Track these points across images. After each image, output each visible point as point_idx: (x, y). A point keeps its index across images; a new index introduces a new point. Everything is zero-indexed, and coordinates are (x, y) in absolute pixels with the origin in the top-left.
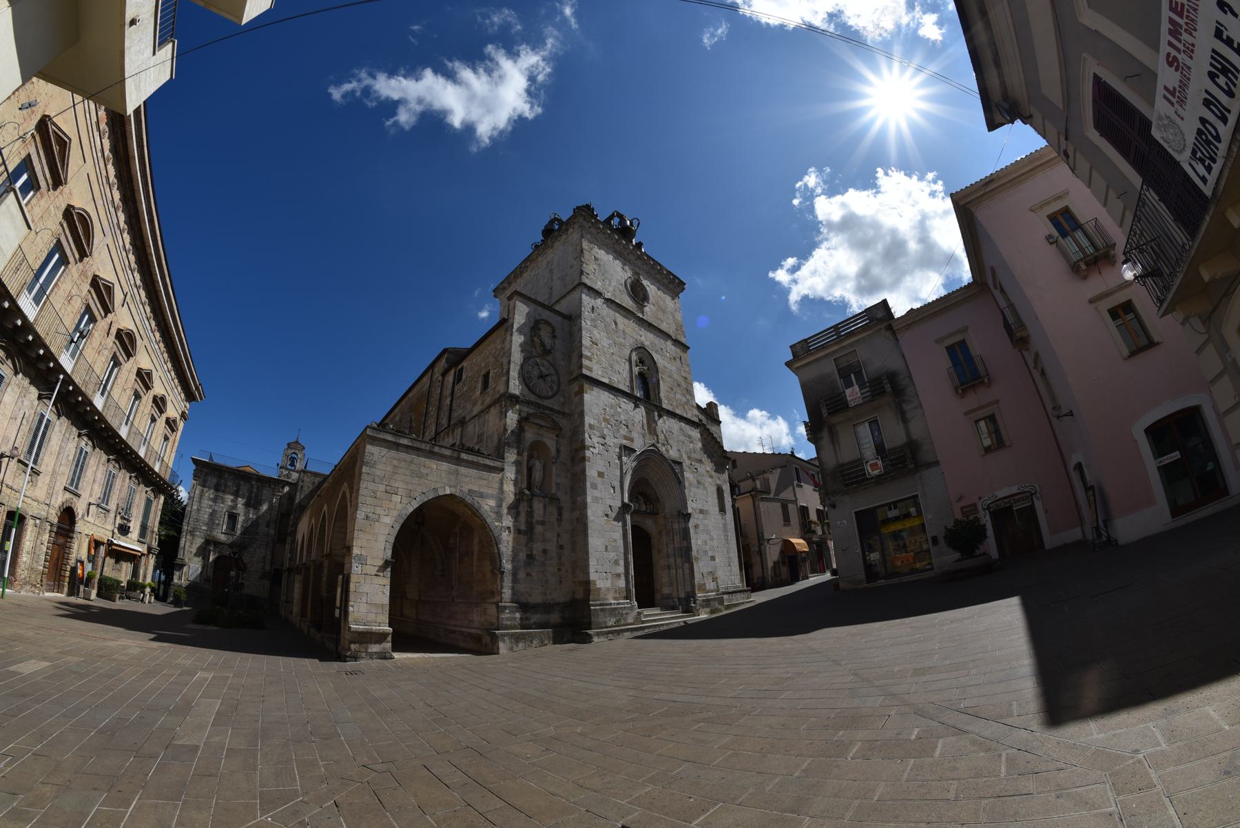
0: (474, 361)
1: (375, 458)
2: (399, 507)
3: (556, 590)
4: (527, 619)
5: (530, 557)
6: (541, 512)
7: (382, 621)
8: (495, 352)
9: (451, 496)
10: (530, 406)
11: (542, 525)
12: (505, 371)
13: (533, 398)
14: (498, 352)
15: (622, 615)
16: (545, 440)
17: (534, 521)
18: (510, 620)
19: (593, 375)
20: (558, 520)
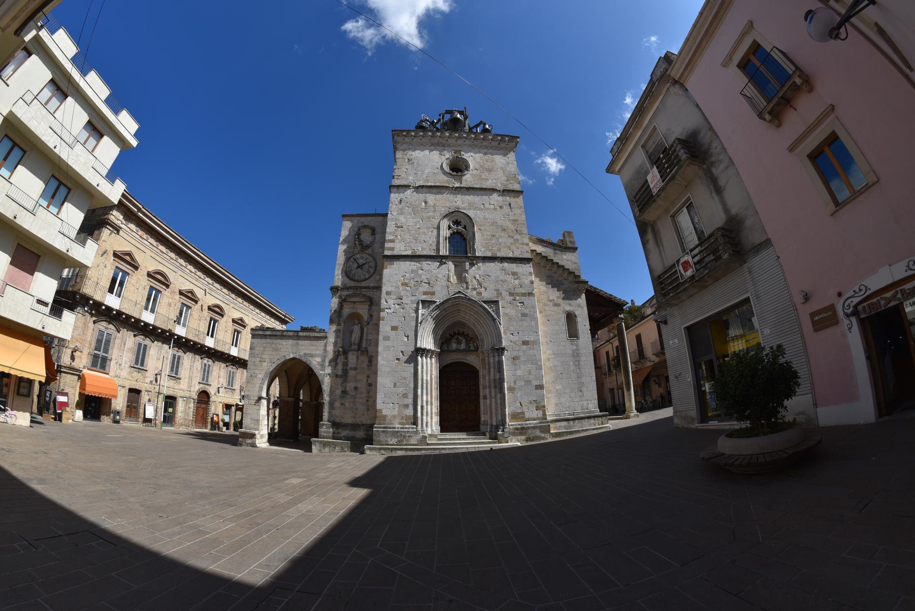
2: (266, 368)
3: (363, 415)
4: (338, 433)
5: (344, 392)
6: (355, 361)
9: (294, 359)
10: (350, 290)
11: (355, 370)
13: (352, 284)
15: (405, 437)
16: (359, 311)
17: (348, 368)
18: (326, 433)
19: (396, 253)
20: (368, 365)
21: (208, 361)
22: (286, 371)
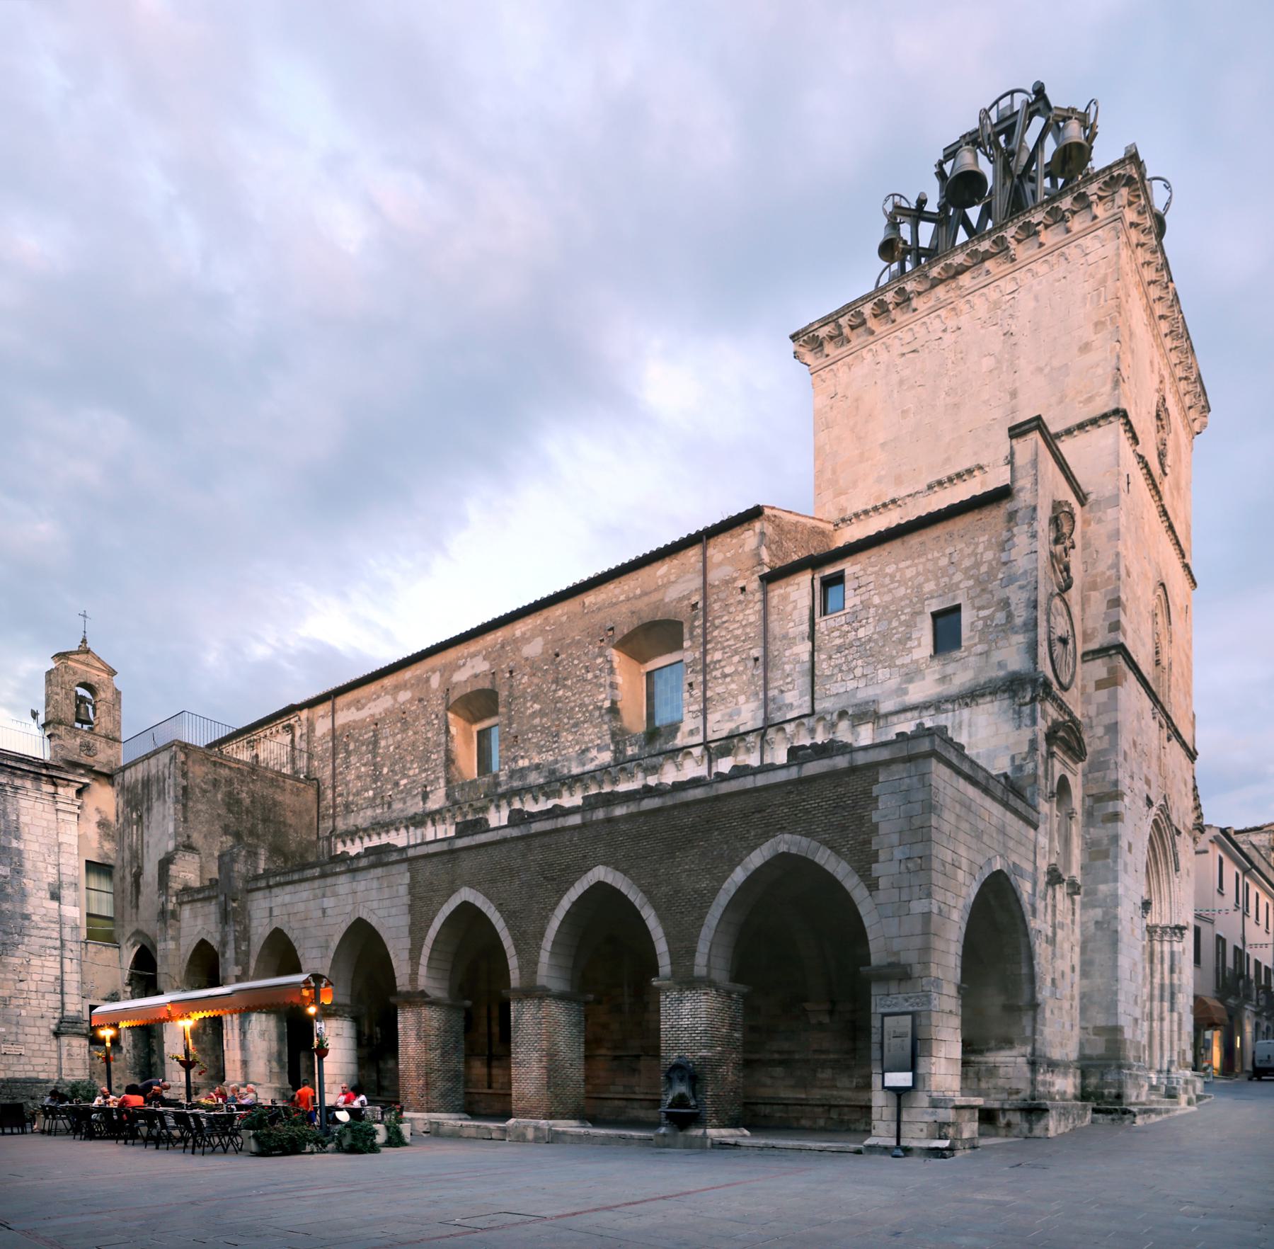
0: (890, 569)
8: (977, 565)
12: (1018, 621)
14: (984, 569)
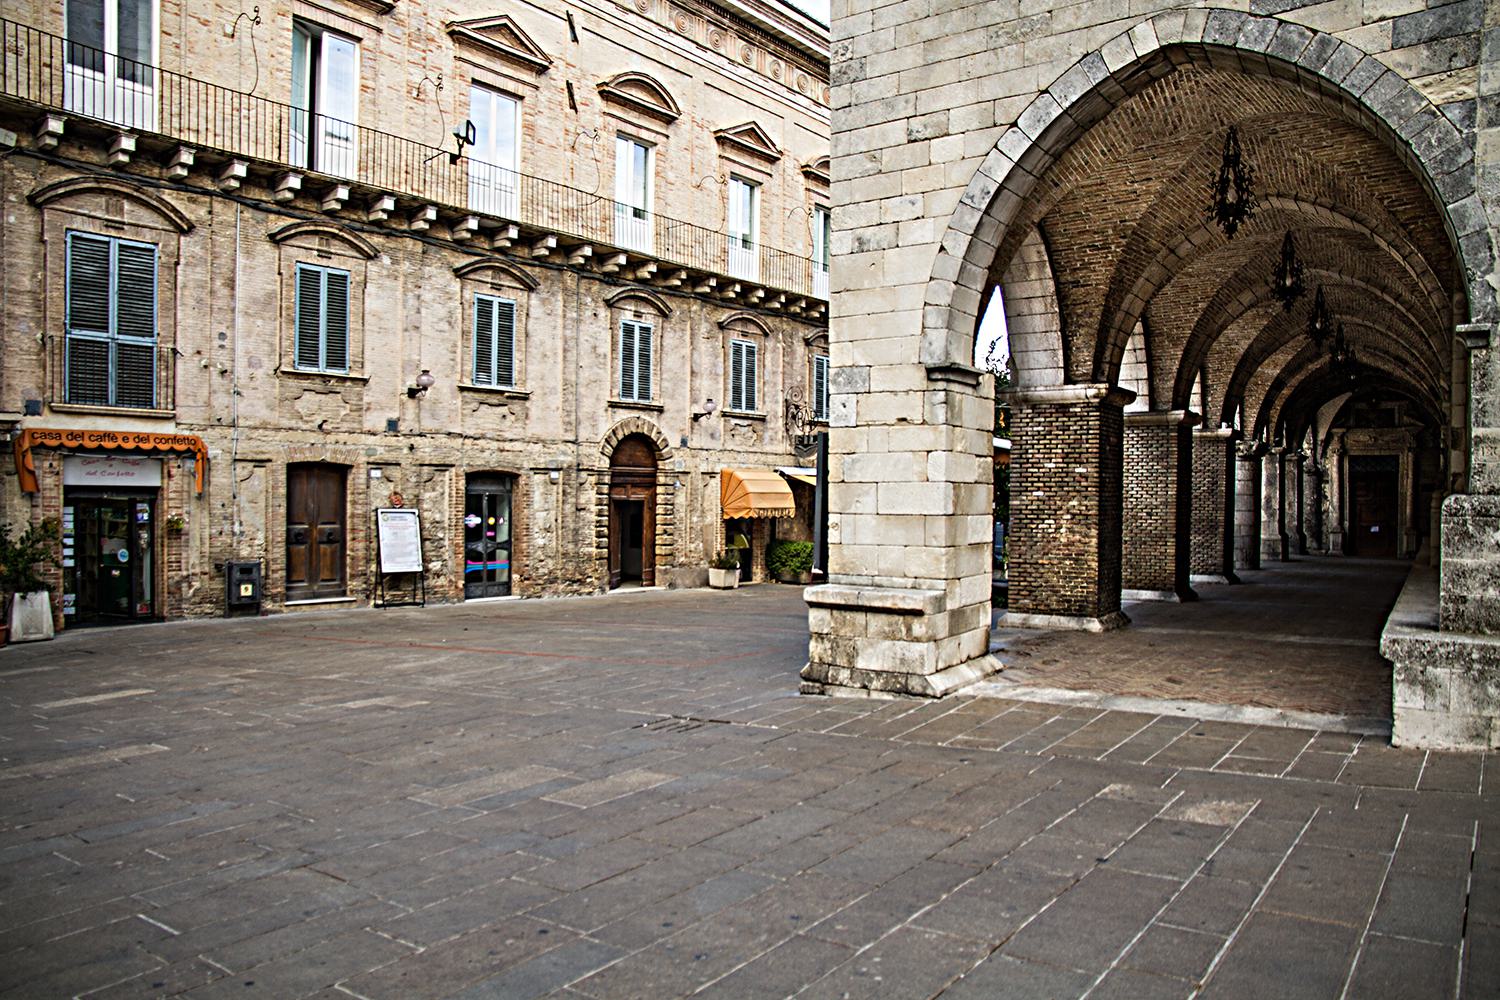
1: (861, 48)
2: (959, 174)
7: (922, 572)
21: (638, 315)
22: (1042, 228)
